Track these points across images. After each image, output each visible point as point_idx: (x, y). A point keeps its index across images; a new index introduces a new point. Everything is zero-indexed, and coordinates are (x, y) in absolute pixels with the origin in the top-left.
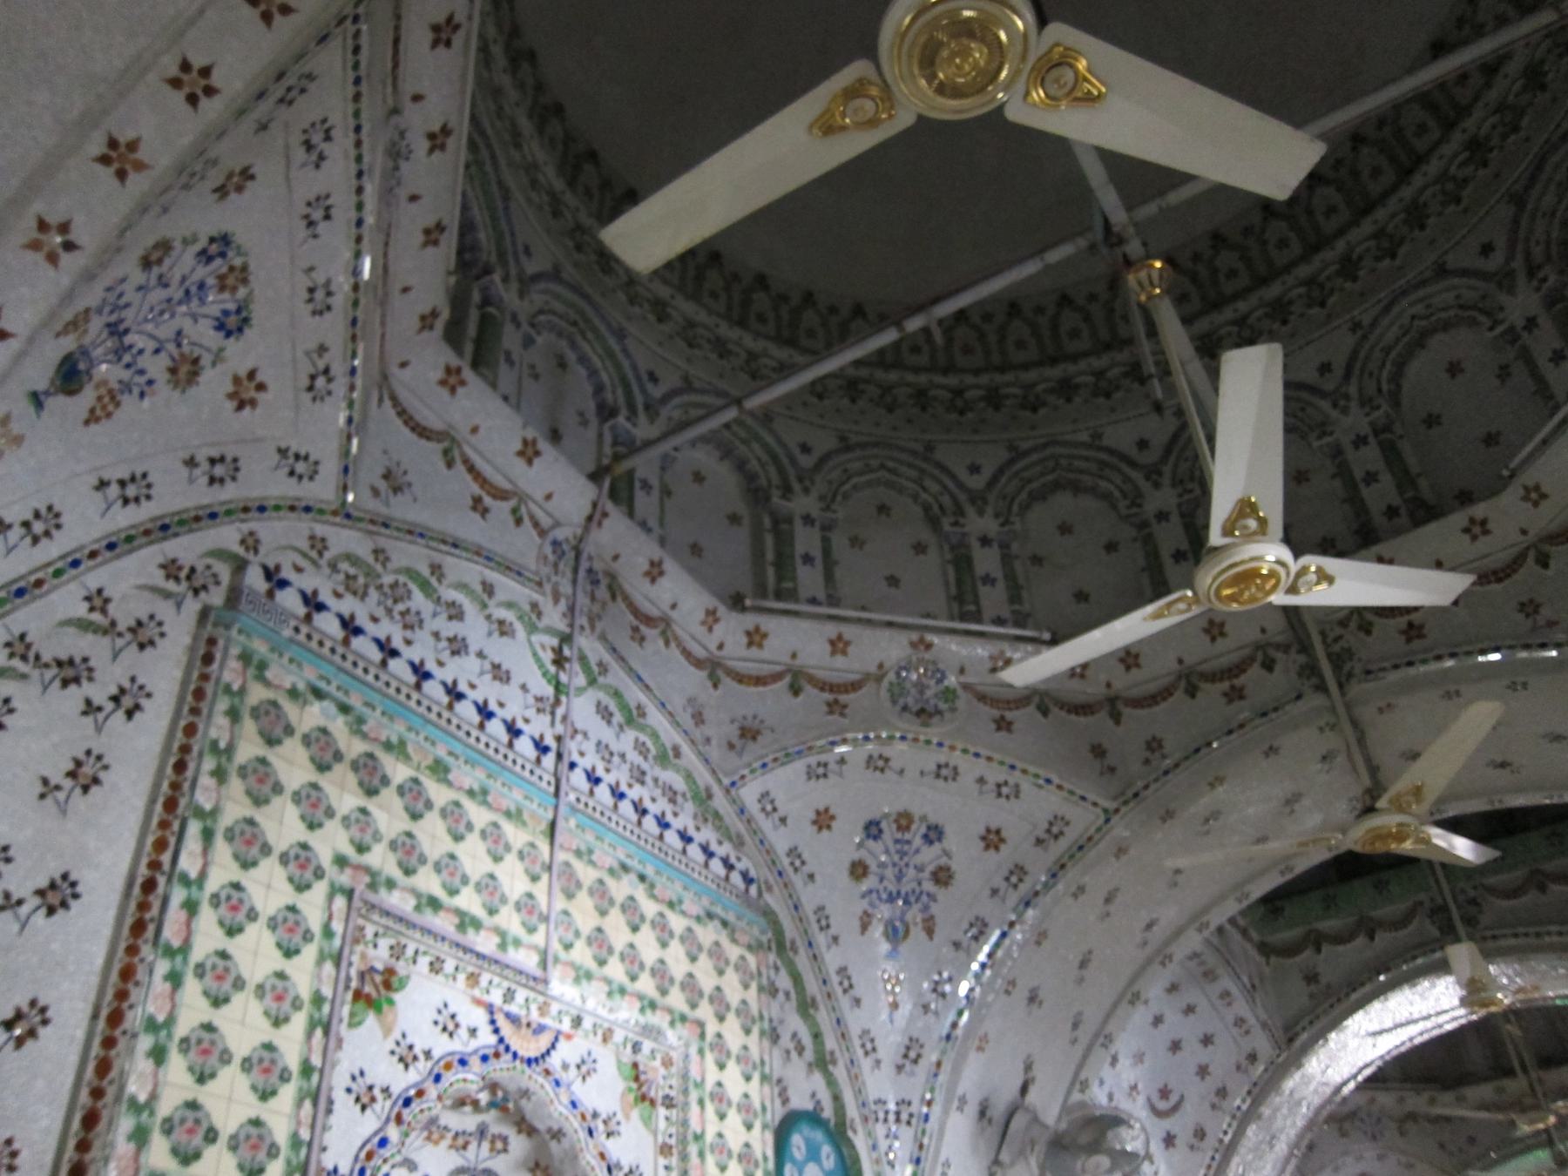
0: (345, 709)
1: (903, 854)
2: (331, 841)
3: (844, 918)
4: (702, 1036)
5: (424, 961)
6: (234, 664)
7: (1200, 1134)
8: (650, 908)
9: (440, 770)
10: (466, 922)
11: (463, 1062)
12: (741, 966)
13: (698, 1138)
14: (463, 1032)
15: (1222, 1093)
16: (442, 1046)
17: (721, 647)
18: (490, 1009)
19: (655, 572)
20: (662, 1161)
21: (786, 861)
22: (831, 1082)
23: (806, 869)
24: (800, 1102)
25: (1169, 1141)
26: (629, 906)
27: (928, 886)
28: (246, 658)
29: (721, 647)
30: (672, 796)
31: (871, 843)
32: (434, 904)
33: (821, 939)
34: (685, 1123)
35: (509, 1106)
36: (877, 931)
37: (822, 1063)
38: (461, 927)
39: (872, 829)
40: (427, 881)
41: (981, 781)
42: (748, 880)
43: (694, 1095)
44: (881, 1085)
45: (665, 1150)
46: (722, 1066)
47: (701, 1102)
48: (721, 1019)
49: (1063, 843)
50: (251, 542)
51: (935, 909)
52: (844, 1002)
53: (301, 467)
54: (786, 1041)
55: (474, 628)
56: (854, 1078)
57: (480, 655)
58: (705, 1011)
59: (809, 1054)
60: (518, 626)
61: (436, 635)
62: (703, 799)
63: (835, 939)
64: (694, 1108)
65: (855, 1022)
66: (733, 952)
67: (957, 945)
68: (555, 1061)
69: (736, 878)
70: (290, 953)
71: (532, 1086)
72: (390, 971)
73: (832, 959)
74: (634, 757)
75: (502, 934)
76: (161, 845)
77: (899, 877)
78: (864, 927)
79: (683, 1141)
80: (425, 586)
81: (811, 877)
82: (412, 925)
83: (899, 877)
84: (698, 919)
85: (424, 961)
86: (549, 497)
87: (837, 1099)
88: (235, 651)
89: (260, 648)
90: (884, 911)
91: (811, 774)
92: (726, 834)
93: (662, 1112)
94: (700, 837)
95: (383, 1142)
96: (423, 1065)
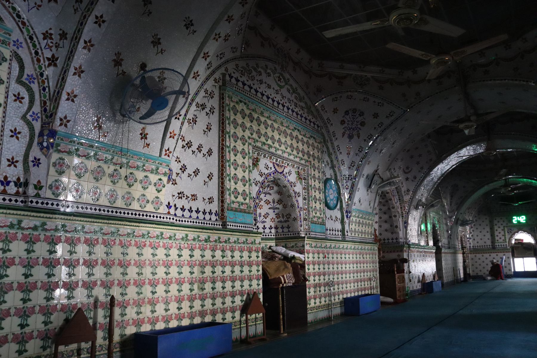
0: (245, 104)
1: (353, 118)
2: (247, 133)
3: (339, 135)
4: (311, 164)
5: (263, 155)
6: (227, 99)
7: (415, 178)
8: (300, 137)
9: (262, 114)
10: (270, 146)
11: (270, 175)
12: (317, 148)
13: (311, 186)
14: (269, 169)
15: (422, 168)
16: (266, 172)
17: (312, 67)
18: (274, 163)
19: (298, 52)
20: (304, 191)
21: (326, 121)
22: (334, 171)
23: (331, 123)
24: (328, 176)
25: (407, 179)
26: (297, 137)
27: (359, 126)
28: (228, 97)
29: (312, 67)
30: (302, 108)
31: (346, 116)
32: (264, 144)
33: (334, 139)
34: (308, 183)
35: (276, 182)
36: (346, 136)
37: (333, 167)
38: (269, 148)
39: (347, 113)
40: (263, 139)
41: (374, 102)
42: (318, 127)
43: (309, 178)
44: (345, 171)
45: (304, 189)
46: (314, 171)
47: (311, 179)
48: (314, 160)
49: (393, 118)
50: (226, 70)
51: (360, 132)
52: (338, 153)
53: (235, 50)
54: (325, 163)
55: (264, 77)
56: (339, 170)
57: (265, 83)
58: (311, 159)
59: (330, 165)
60: (271, 73)
61: (257, 80)
62: (309, 108)
63: (337, 138)
64: (310, 180)
65: (340, 157)
66: (316, 144)
67: (365, 140)
68: (285, 172)
69: (316, 126)
70: (244, 158)
71: (281, 178)
72: (257, 158)
73: (336, 144)
74: (295, 101)
75: (275, 148)
76: (223, 140)
77: (352, 124)
78: (343, 136)
79: (308, 187)
80: (255, 69)
81: (332, 124)
82: (261, 149)
83: (352, 124)
84: (309, 138)
85: (263, 155)
86: (276, 38)
87: (336, 175)
88: (227, 96)
89: (231, 93)
90: (348, 132)
91: (333, 100)
92: (314, 116)
93: (303, 181)
94: (309, 118)
95: (260, 191)
96: (264, 176)
